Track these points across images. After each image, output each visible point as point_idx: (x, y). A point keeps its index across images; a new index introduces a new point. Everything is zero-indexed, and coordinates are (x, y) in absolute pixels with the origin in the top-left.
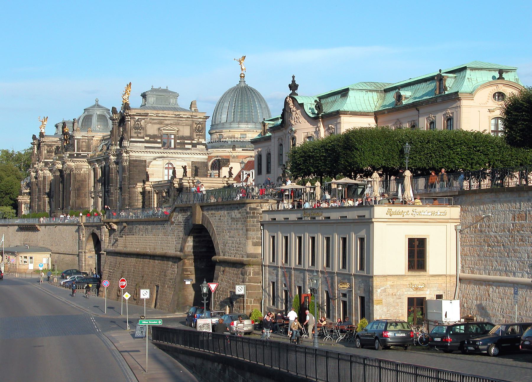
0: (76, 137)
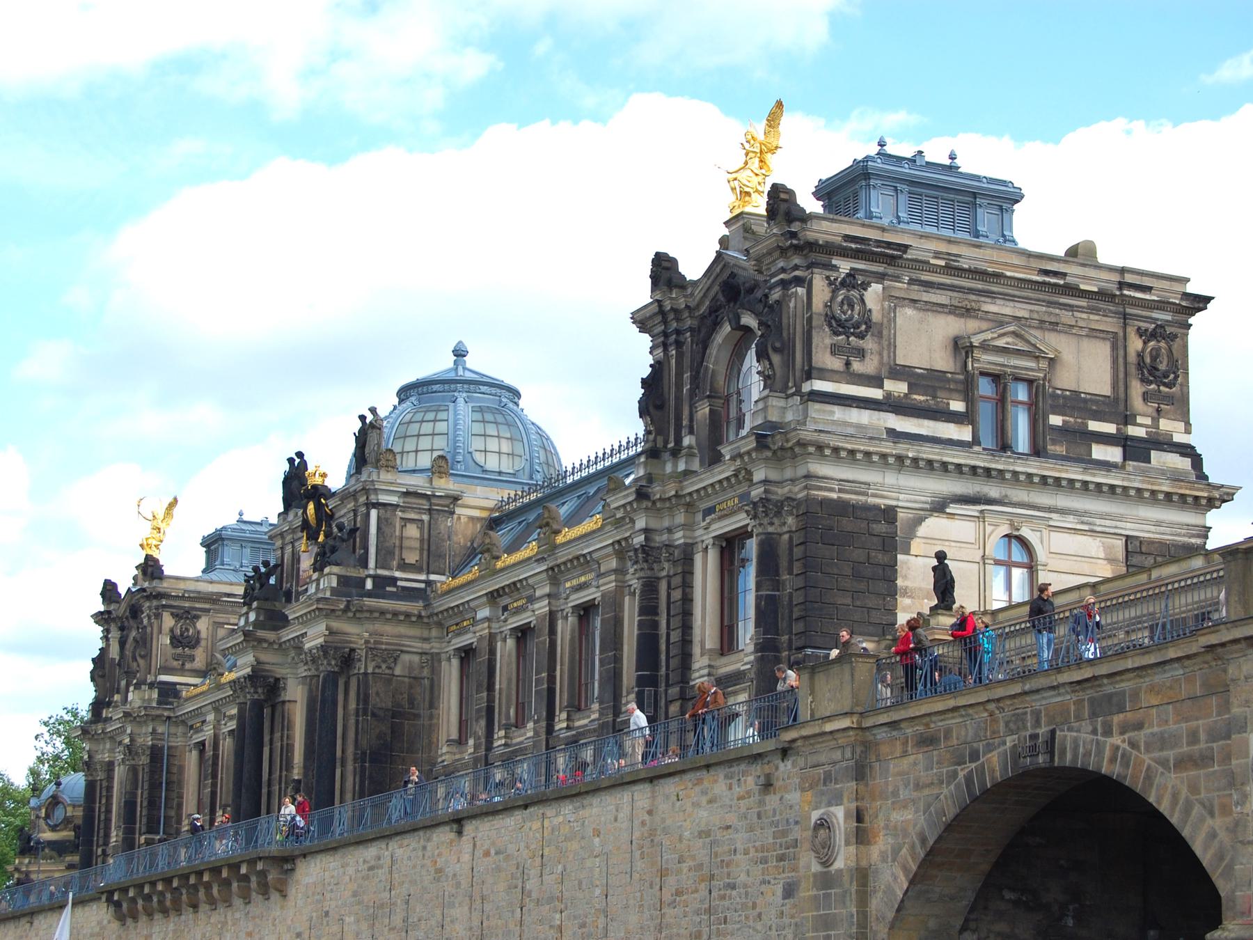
0: (373, 498)
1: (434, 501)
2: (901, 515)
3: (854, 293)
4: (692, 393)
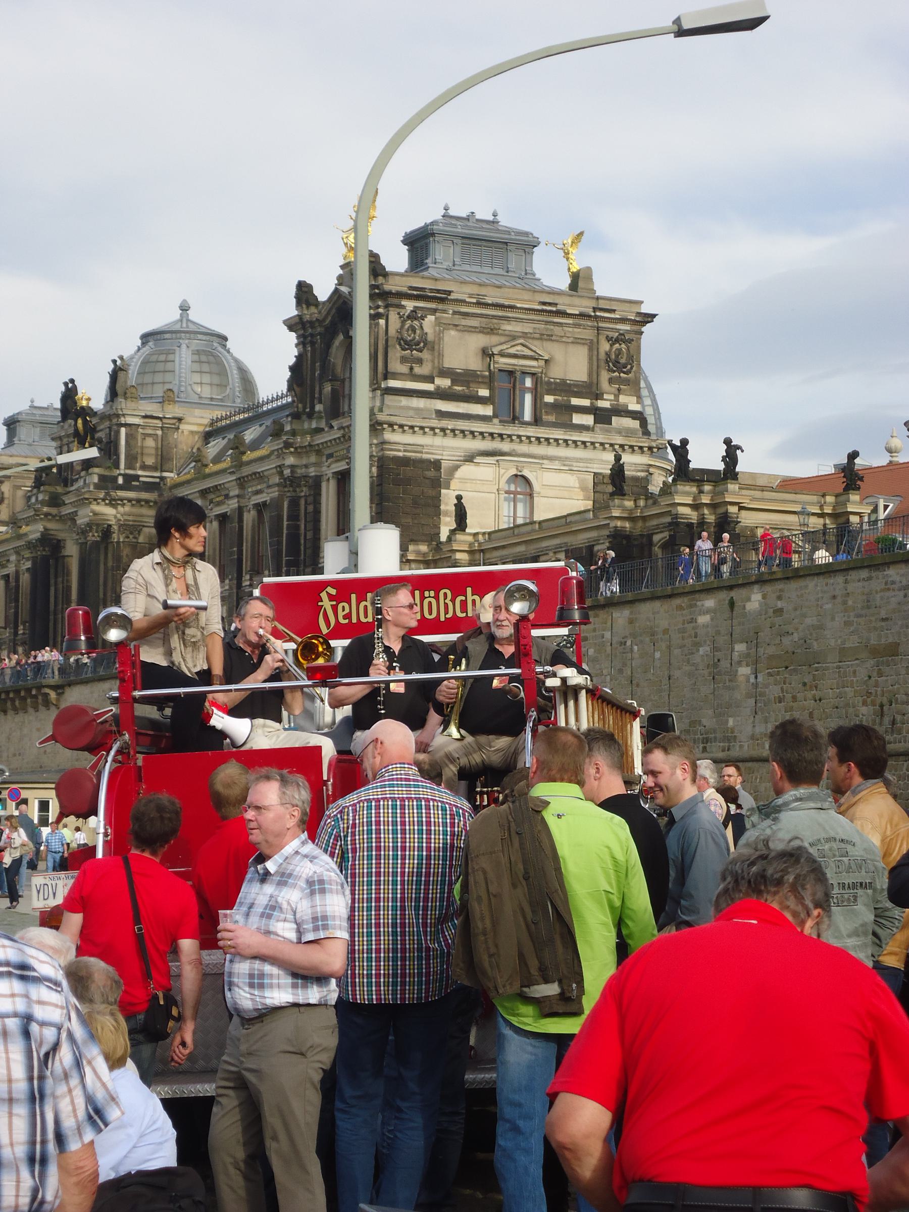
0: (123, 420)
1: (165, 421)
2: (444, 464)
3: (416, 323)
4: (321, 376)
